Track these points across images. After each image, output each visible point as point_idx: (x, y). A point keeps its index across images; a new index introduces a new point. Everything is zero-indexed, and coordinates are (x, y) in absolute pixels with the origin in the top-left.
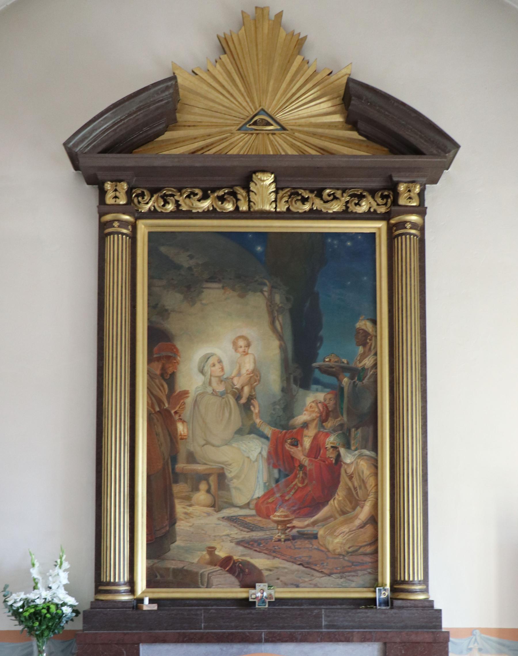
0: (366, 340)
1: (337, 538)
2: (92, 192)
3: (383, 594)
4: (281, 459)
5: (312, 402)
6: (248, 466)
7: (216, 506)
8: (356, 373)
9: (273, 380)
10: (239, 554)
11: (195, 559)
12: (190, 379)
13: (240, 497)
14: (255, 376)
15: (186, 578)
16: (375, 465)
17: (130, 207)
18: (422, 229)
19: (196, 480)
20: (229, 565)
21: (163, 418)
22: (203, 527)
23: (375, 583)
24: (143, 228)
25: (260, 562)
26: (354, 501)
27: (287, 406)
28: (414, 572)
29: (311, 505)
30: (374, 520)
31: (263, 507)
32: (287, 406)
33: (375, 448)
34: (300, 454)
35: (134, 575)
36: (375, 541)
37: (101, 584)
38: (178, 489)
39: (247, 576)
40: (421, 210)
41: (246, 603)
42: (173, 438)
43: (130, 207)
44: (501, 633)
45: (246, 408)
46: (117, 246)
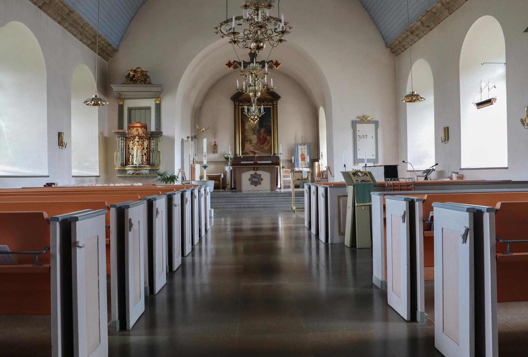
0: (270, 122)
1: (266, 148)
2: (233, 103)
3: (272, 155)
4: (258, 138)
5: (263, 130)
6: (254, 138)
7: (250, 144)
8: (268, 126)
9: (258, 127)
10: (253, 150)
11: (248, 151)
12: (247, 127)
13: (253, 143)
14: (255, 127)
15: (247, 153)
16: (271, 138)
17: (239, 105)
18: (277, 107)
19: (247, 141)
20: (253, 152)
21: (243, 133)
22: (249, 147)
23: (271, 154)
24: (240, 107)
25: (256, 151)
26: (268, 143)
27: (259, 131)
28: (276, 152)
29: (263, 144)
30: (271, 146)
31: (256, 144)
32: (259, 131)
33: (271, 136)
34: (261, 137)
35: (239, 152)
36: (271, 148)
37: (236, 154)
38: (245, 142)
39: (255, 153)
40: (277, 104)
41: (254, 157)
42: (244, 135)
43: (239, 105)
44: (288, 160)
45: (254, 131)
46: (237, 110)
